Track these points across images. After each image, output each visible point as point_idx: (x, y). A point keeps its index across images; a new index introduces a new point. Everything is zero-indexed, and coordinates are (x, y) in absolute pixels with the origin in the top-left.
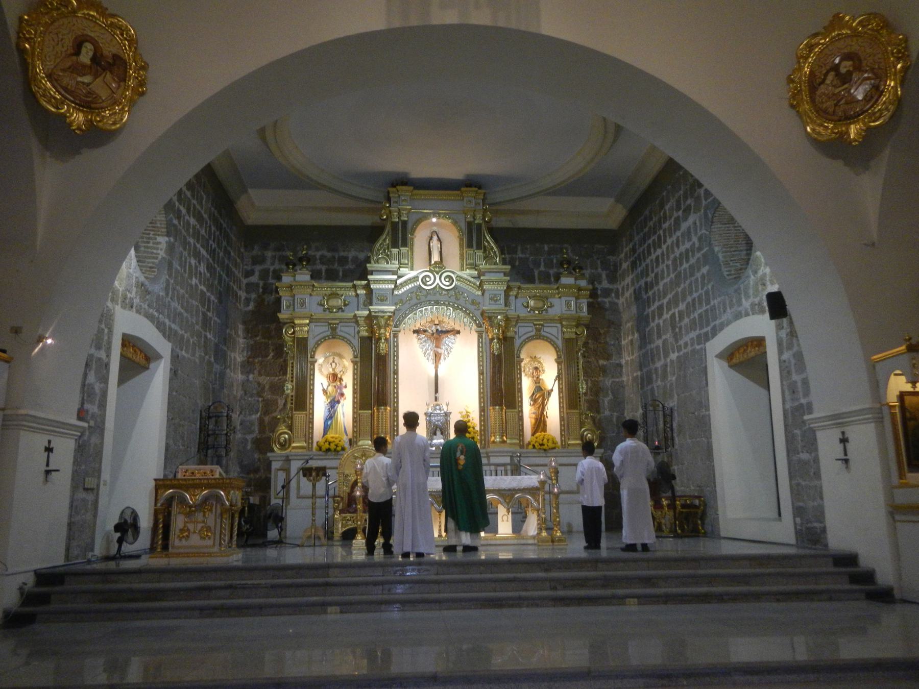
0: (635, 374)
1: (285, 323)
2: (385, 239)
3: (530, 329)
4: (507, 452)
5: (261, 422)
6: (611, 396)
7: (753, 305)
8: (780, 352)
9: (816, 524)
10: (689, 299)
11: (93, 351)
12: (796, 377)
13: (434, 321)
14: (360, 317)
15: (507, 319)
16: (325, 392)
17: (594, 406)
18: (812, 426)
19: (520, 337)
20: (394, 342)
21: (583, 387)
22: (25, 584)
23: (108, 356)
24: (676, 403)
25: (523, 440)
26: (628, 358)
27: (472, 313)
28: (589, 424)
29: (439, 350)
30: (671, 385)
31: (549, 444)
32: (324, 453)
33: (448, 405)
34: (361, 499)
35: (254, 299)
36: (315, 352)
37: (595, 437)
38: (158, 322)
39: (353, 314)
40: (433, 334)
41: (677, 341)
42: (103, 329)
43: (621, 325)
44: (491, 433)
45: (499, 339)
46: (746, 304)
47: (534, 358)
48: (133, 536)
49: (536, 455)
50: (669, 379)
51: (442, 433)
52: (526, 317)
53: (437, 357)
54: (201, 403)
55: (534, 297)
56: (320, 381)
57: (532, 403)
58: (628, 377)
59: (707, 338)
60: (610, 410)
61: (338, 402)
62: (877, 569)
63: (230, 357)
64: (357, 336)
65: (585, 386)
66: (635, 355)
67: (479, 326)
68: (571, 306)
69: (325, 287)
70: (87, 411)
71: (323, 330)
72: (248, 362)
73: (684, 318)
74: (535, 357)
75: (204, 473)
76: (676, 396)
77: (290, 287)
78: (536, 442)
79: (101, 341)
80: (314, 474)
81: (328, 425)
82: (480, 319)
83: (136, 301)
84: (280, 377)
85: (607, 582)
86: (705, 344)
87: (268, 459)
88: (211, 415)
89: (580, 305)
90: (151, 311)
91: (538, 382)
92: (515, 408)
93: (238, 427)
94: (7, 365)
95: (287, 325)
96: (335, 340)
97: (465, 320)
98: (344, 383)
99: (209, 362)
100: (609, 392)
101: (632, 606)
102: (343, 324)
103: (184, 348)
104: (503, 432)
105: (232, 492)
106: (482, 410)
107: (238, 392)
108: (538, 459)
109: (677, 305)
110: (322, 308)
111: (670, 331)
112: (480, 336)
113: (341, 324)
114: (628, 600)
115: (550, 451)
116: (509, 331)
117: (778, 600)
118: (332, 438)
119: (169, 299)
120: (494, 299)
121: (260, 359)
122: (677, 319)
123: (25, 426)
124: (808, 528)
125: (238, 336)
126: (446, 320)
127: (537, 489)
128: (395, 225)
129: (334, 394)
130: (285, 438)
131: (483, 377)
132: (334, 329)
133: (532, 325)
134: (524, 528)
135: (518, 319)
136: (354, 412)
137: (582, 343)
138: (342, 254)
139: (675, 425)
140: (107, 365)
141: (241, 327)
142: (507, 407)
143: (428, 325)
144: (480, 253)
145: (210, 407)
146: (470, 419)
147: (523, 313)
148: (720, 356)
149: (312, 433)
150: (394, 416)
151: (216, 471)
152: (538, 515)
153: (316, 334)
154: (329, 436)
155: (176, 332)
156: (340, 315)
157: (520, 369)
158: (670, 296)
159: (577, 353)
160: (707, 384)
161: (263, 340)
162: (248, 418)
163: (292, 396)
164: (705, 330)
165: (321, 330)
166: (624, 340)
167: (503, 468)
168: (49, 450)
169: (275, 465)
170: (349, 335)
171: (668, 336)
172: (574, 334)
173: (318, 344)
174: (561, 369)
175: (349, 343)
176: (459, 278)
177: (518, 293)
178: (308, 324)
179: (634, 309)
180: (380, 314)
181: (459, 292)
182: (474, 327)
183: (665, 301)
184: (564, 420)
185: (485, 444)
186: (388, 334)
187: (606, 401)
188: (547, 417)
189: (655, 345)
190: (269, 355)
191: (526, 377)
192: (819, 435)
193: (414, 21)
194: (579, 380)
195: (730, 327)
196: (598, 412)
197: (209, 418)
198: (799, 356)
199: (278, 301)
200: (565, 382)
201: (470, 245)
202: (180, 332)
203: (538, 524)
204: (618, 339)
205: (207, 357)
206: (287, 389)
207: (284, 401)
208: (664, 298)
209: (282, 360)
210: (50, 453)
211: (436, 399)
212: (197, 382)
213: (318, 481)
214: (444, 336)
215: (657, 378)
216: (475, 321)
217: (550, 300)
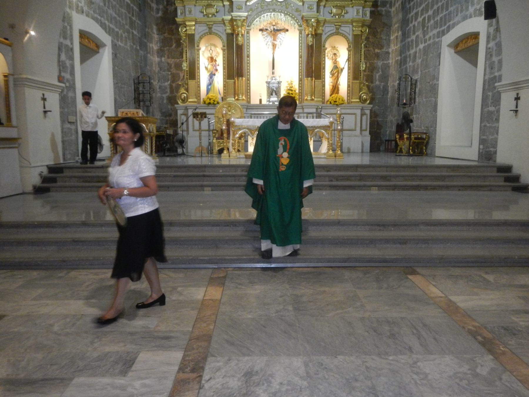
0: (397, 58)
1: (180, 25)
3: (332, 28)
4: (314, 106)
5: (171, 87)
6: (381, 73)
7: (475, 10)
8: (488, 42)
9: (492, 149)
10: (435, 7)
11: (62, 40)
12: (495, 59)
13: (272, 23)
14: (226, 20)
15: (318, 22)
16: (206, 68)
17: (370, 79)
18: (499, 90)
19: (325, 34)
20: (247, 36)
21: (363, 67)
22: (42, 172)
23: (72, 44)
24: (419, 77)
25: (324, 99)
26: (394, 48)
27: (296, 18)
28: (365, 90)
29: (275, 42)
30: (418, 65)
31: (340, 101)
32: (206, 105)
33: (280, 77)
34: (226, 131)
35: (162, 9)
36: (199, 43)
37: (368, 98)
38: (101, 23)
39: (222, 18)
40: (271, 32)
41: (424, 36)
42: (66, 27)
43: (391, 26)
44: (305, 94)
45: (312, 35)
46: (471, 10)
47: (334, 48)
48: (100, 150)
49: (331, 108)
50: (417, 61)
51: (276, 94)
52: (330, 20)
53: (274, 46)
54: (133, 74)
55: (336, 7)
56: (203, 62)
57: (331, 76)
58: (393, 60)
59: (443, 33)
60: (379, 81)
61: (214, 75)
62: (522, 174)
63: (149, 46)
64: (224, 33)
65: (364, 66)
66: (398, 46)
68: (359, 13)
70: (64, 77)
71: (204, 29)
72: (161, 50)
73: (430, 20)
74: (335, 47)
75: (133, 114)
76: (420, 72)
78: (332, 100)
79: (66, 33)
80: (199, 116)
81: (209, 89)
82: (301, 21)
83: (85, 9)
84: (180, 59)
85: (362, 178)
86: (441, 38)
87: (176, 108)
88: (140, 82)
89: (365, 12)
90: (96, 15)
91: (335, 62)
92: (320, 79)
93: (158, 90)
94: (9, 48)
95: (181, 26)
96: (211, 36)
97: (292, 22)
98: (217, 63)
99: (136, 49)
100: (380, 70)
101: (374, 191)
102: (216, 25)
103: (120, 40)
105: (150, 125)
106: (300, 80)
107: (156, 69)
108: (333, 110)
109: (427, 11)
110: (202, 14)
111: (421, 30)
112: (300, 33)
113: (215, 25)
114: (372, 188)
115: (340, 105)
116: (319, 29)
117: (459, 190)
118: (212, 96)
119: (106, 8)
120: (310, 8)
121: (168, 48)
122: (427, 21)
123: (26, 85)
124: (486, 151)
125: (154, 33)
126: (279, 22)
127: (328, 127)
129: (211, 70)
130: (185, 96)
131: (302, 60)
132: (210, 28)
133: (333, 25)
134: (320, 149)
136: (224, 81)
137: (365, 38)
139: (417, 90)
140: (72, 49)
141: (155, 27)
142: (315, 79)
143: (268, 25)
145: (139, 77)
146: (293, 85)
147: (328, 18)
148: (449, 46)
149: (200, 93)
150: (248, 83)
151: (139, 113)
152: (328, 142)
153: (199, 32)
154: (210, 95)
155: (113, 30)
156: (214, 19)
157: (325, 55)
158: (423, 5)
159: (361, 44)
160: (439, 65)
161: (169, 36)
162: (163, 84)
163: (187, 71)
164: (443, 28)
165: (203, 28)
166: (392, 36)
167: (311, 115)
168: (44, 99)
169: (180, 112)
170: (220, 32)
171: (419, 33)
172: (360, 31)
173: (201, 38)
174: (350, 55)
175: (220, 37)
177: (326, 4)
178: (194, 25)
179: (400, 16)
180: (238, 18)
181: (288, 3)
183: (420, 9)
184: (350, 87)
185: (301, 101)
186: (243, 31)
187: (377, 76)
188: (340, 85)
189: (411, 39)
190: (171, 46)
191: (328, 60)
192: (503, 96)
194: (361, 61)
195: (459, 25)
196: (372, 82)
197: (139, 83)
198: (499, 45)
199: (176, 10)
200: (352, 63)
202: (116, 30)
203: (328, 147)
204: (388, 35)
205: (135, 46)
206: (184, 67)
207: (183, 74)
208: (420, 6)
209: (180, 49)
210: (45, 101)
211: (273, 73)
212: (130, 61)
213: (202, 120)
214: (278, 33)
215: (410, 61)
216: (298, 23)
217: (346, 8)
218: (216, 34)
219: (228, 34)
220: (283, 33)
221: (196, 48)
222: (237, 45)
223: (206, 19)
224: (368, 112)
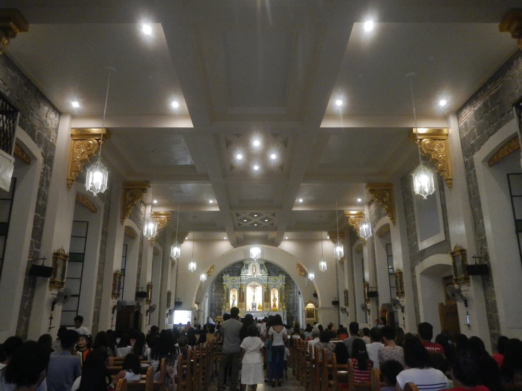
2: (244, 266)
5: (218, 303)
16: (232, 299)
21: (283, 298)
29: (255, 290)
45: (266, 289)
47: (274, 292)
53: (254, 291)
55: (274, 279)
58: (295, 294)
67: (262, 286)
69: (232, 278)
77: (225, 278)
91: (274, 296)
98: (236, 297)
104: (267, 307)
106: (263, 303)
107: (214, 297)
112: (262, 288)
120: (265, 280)
128: (246, 265)
132: (234, 286)
135: (270, 284)
138: (236, 267)
144: (263, 270)
156: (235, 283)
159: (282, 290)
165: (231, 286)
173: (231, 289)
175: (237, 289)
176: (258, 276)
187: (291, 300)
190: (219, 289)
197: (212, 305)
201: (261, 269)
220: (257, 287)
221: (229, 292)
222: (242, 292)
223: (232, 283)
224: (286, 313)
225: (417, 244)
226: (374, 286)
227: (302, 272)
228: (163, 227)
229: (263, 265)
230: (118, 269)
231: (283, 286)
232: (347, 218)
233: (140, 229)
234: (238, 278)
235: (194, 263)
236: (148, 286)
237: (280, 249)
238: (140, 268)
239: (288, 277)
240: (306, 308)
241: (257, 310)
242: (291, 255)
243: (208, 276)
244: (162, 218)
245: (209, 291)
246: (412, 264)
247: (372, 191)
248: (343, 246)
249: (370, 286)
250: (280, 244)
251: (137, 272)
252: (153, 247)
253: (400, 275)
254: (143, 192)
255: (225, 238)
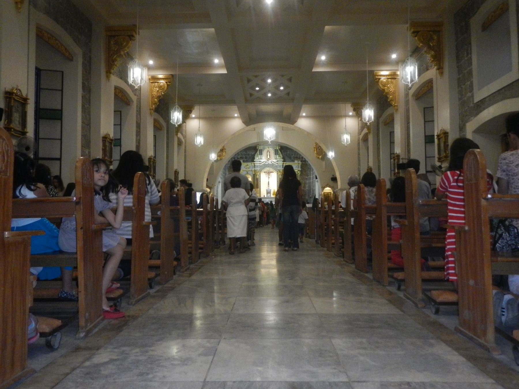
2: (258, 152)
6: (308, 185)
26: (311, 177)
29: (269, 176)
45: (281, 175)
53: (269, 178)
58: (311, 181)
67: (277, 172)
120: (280, 166)
128: (260, 150)
132: (247, 172)
138: (248, 153)
156: (249, 169)
175: (251, 175)
176: (273, 162)
182: (276, 172)
193: (261, 141)
196: (305, 188)
201: (275, 154)
218: (249, 174)
219: (253, 174)
220: (272, 173)
222: (256, 178)
225: (472, 96)
226: (405, 157)
227: (320, 155)
228: (163, 94)
229: (278, 150)
230: (107, 133)
231: (299, 172)
232: (378, 80)
233: (135, 95)
234: (252, 164)
235: (201, 137)
236: (149, 160)
237: (297, 127)
238: (139, 140)
239: (304, 163)
240: (323, 192)
241: (272, 196)
242: (308, 134)
243: (219, 156)
244: (161, 83)
245: (221, 176)
246: (461, 123)
247: (416, 33)
248: (373, 109)
249: (401, 157)
250: (297, 121)
251: (136, 143)
252: (153, 118)
253: (445, 136)
254: (131, 40)
255: (236, 115)
